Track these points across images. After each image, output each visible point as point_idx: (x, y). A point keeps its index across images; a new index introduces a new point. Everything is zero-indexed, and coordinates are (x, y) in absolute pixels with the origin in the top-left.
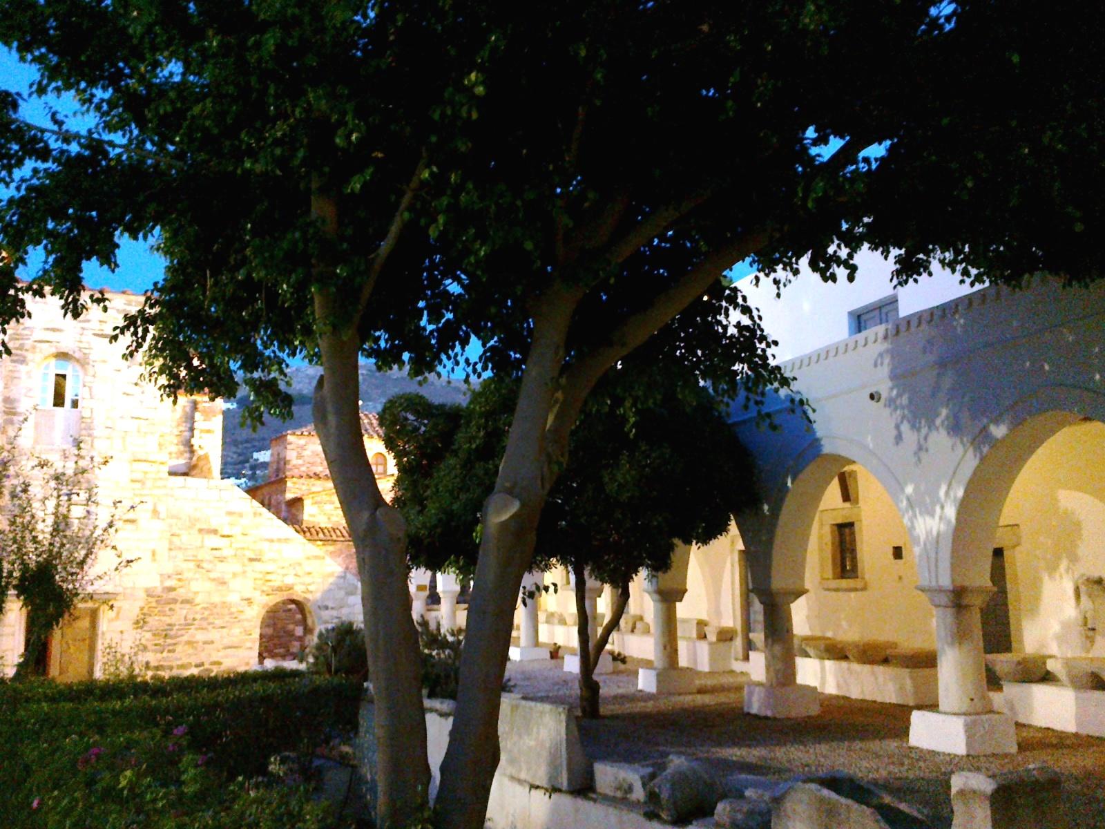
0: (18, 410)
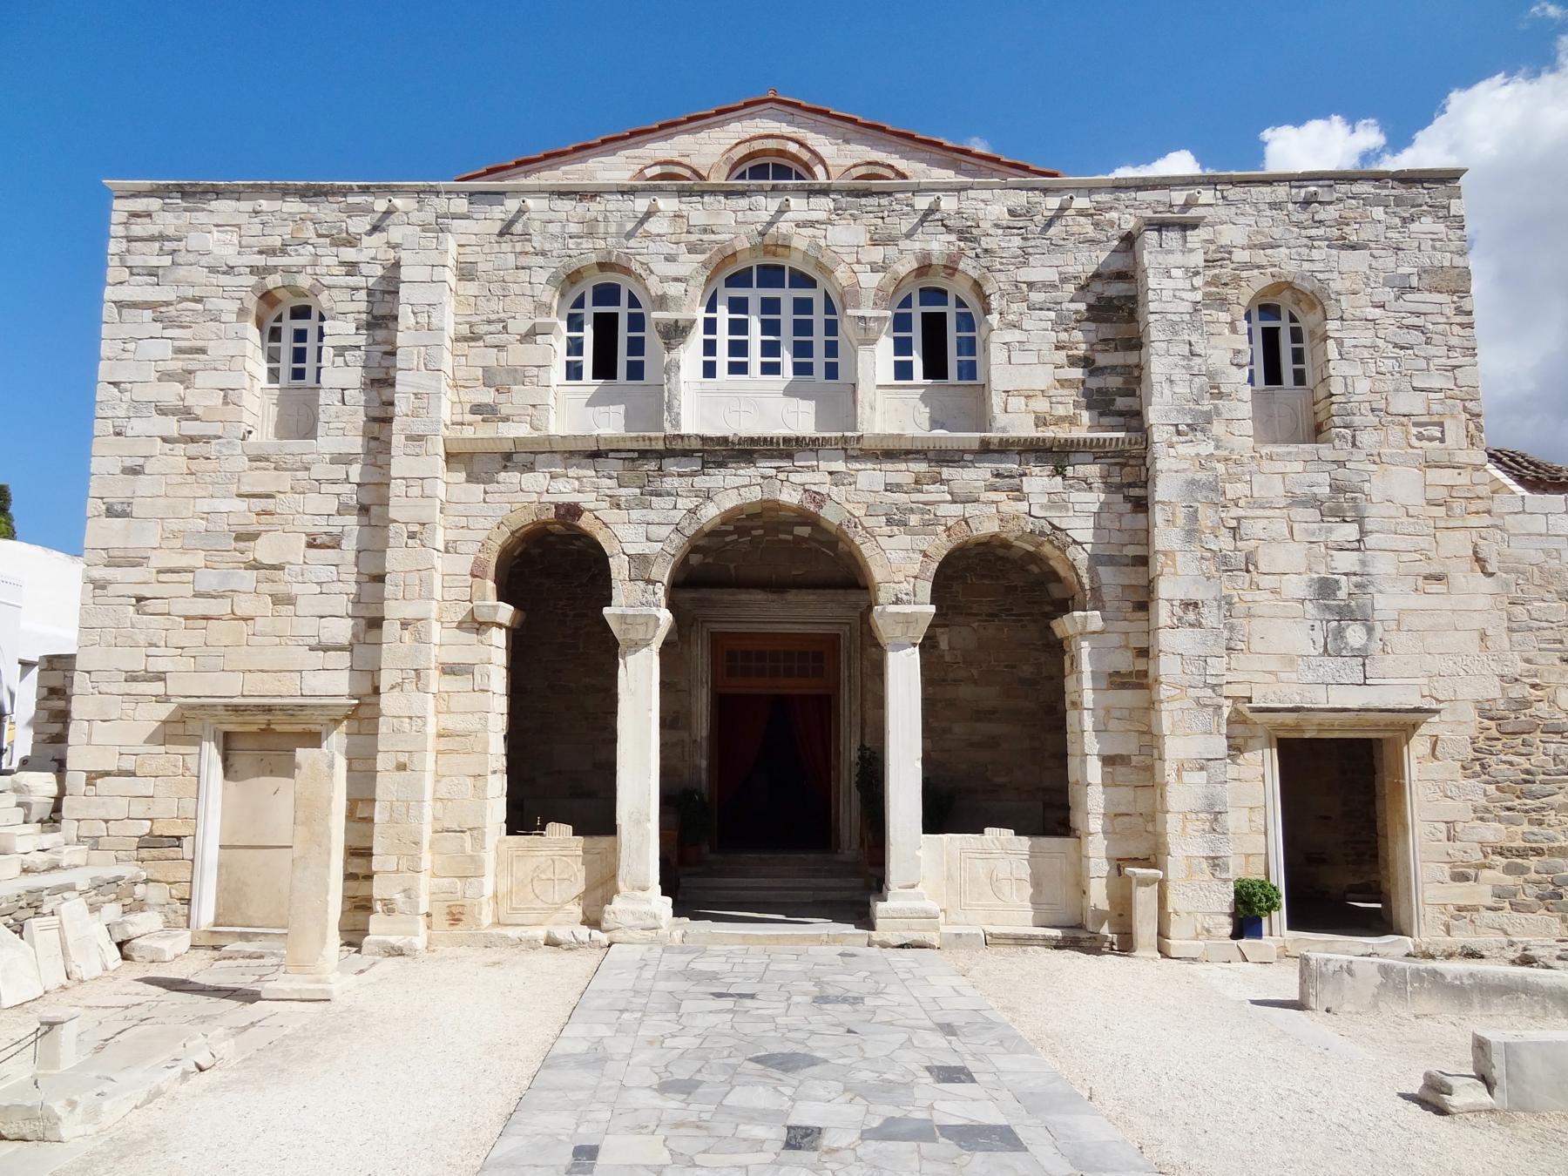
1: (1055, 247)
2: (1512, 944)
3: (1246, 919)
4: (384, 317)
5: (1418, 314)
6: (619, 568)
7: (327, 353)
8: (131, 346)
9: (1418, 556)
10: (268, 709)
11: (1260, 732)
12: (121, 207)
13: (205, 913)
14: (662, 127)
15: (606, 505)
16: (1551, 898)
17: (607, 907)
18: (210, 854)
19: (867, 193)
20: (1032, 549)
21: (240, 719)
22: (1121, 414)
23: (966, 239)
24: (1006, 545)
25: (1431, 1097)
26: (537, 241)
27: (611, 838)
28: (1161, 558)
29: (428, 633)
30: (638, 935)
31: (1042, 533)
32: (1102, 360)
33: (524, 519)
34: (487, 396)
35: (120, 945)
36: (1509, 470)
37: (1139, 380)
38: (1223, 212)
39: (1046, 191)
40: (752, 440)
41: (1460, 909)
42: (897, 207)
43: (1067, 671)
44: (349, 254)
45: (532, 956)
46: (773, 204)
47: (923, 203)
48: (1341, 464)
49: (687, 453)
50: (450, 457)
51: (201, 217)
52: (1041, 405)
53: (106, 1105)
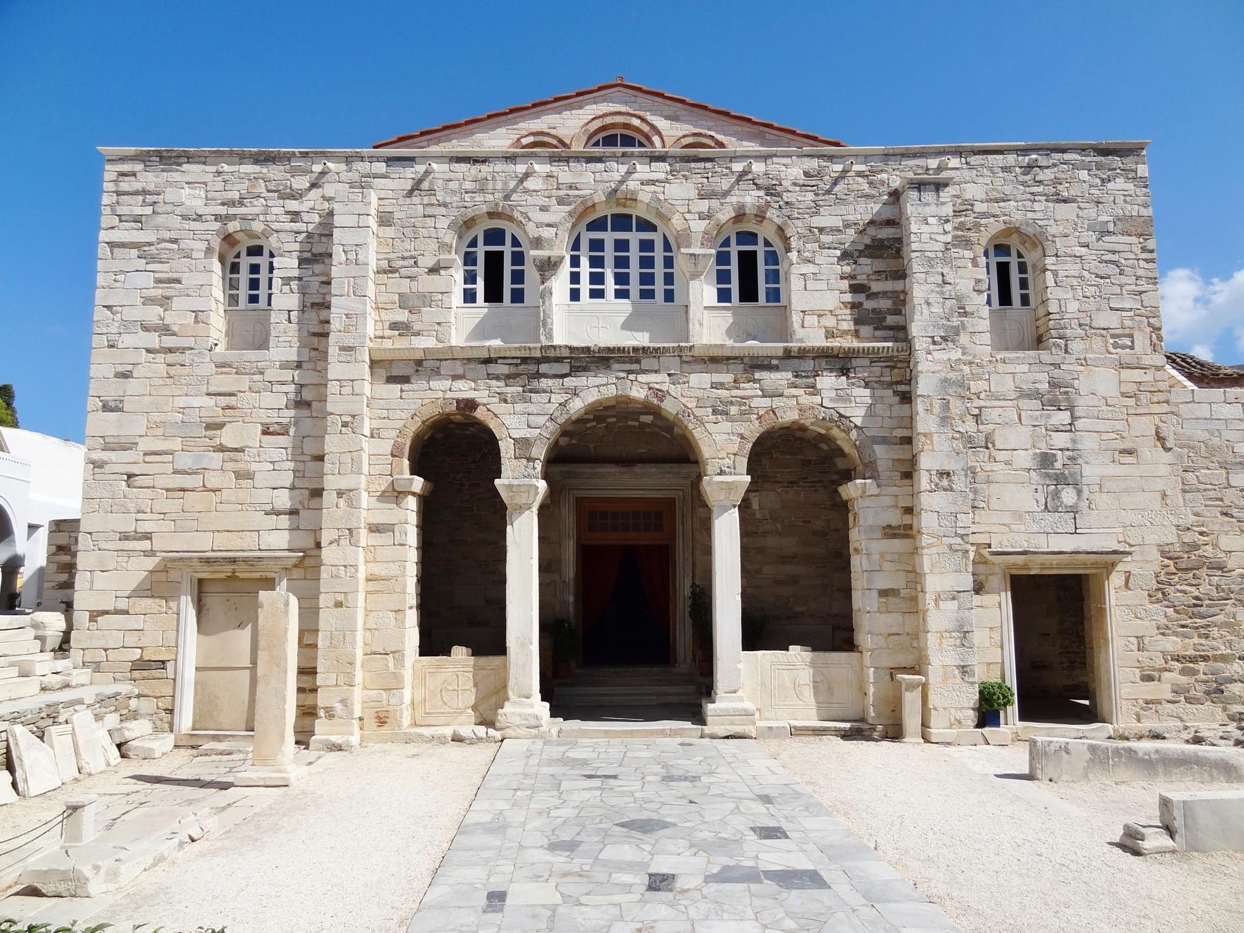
1: (840, 201)
2: (1186, 728)
3: (987, 715)
4: (321, 255)
5: (1114, 252)
6: (506, 449)
7: (277, 283)
8: (121, 277)
9: (1114, 436)
10: (233, 561)
11: (997, 569)
12: (110, 171)
13: (185, 721)
14: (534, 106)
16: (1216, 692)
17: (500, 711)
18: (189, 674)
19: (698, 159)
20: (823, 432)
21: (211, 569)
22: (890, 328)
23: (772, 195)
24: (803, 429)
25: (1129, 842)
26: (440, 196)
27: (502, 658)
28: (922, 439)
29: (359, 500)
30: (524, 731)
31: (831, 420)
32: (876, 287)
33: (432, 411)
34: (402, 316)
35: (119, 746)
36: (1181, 369)
37: (904, 302)
38: (967, 174)
39: (831, 158)
40: (609, 349)
41: (1147, 702)
42: (719, 170)
43: (851, 525)
44: (293, 205)
45: (443, 750)
46: (623, 169)
47: (738, 167)
48: (1057, 366)
49: (558, 360)
50: (374, 364)
51: (176, 176)
52: (830, 322)
53: (123, 868)
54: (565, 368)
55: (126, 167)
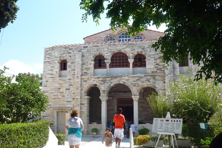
0: (176, 67)
6: (101, 92)
15: (99, 84)
22: (162, 71)
32: (160, 64)
34: (85, 71)
44: (70, 55)
49: (109, 78)
52: (152, 70)
54: (110, 79)
55: (47, 50)
